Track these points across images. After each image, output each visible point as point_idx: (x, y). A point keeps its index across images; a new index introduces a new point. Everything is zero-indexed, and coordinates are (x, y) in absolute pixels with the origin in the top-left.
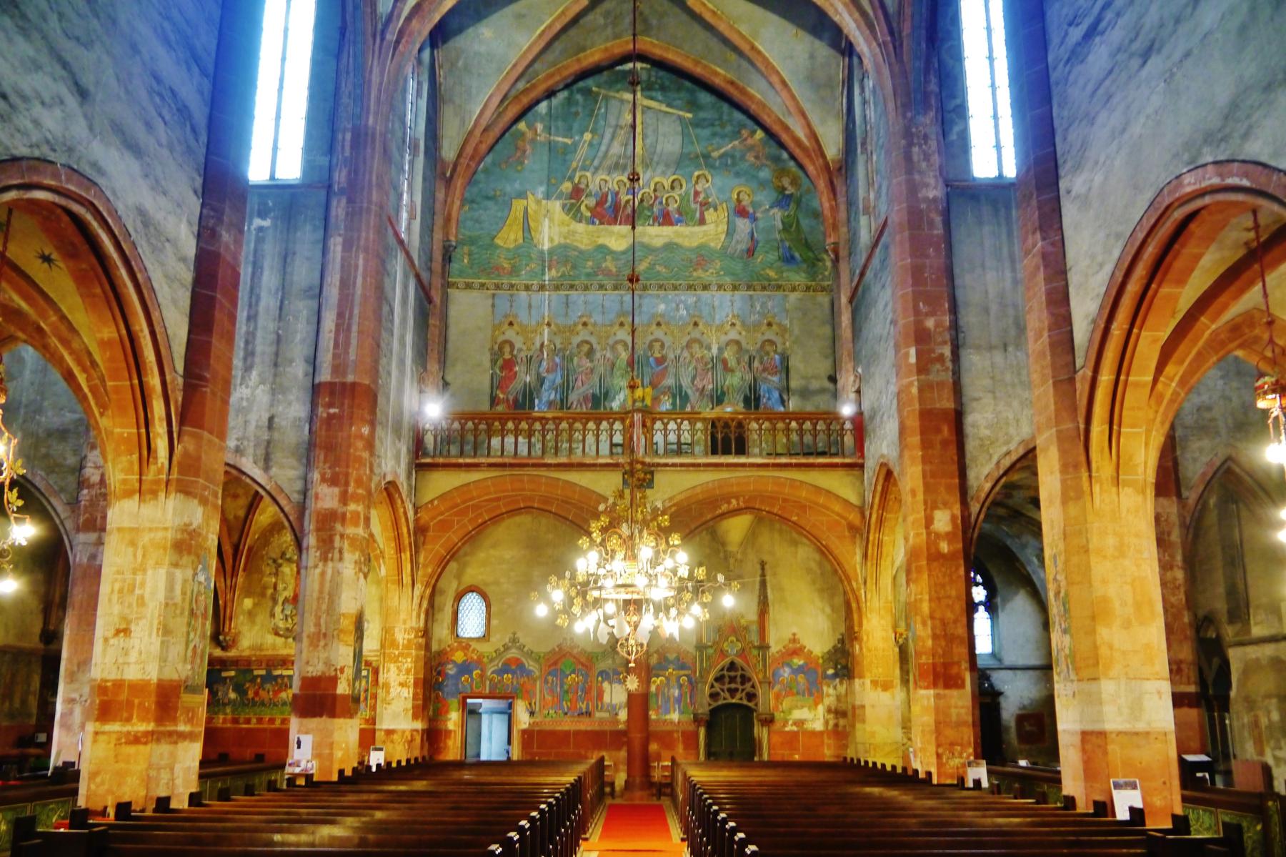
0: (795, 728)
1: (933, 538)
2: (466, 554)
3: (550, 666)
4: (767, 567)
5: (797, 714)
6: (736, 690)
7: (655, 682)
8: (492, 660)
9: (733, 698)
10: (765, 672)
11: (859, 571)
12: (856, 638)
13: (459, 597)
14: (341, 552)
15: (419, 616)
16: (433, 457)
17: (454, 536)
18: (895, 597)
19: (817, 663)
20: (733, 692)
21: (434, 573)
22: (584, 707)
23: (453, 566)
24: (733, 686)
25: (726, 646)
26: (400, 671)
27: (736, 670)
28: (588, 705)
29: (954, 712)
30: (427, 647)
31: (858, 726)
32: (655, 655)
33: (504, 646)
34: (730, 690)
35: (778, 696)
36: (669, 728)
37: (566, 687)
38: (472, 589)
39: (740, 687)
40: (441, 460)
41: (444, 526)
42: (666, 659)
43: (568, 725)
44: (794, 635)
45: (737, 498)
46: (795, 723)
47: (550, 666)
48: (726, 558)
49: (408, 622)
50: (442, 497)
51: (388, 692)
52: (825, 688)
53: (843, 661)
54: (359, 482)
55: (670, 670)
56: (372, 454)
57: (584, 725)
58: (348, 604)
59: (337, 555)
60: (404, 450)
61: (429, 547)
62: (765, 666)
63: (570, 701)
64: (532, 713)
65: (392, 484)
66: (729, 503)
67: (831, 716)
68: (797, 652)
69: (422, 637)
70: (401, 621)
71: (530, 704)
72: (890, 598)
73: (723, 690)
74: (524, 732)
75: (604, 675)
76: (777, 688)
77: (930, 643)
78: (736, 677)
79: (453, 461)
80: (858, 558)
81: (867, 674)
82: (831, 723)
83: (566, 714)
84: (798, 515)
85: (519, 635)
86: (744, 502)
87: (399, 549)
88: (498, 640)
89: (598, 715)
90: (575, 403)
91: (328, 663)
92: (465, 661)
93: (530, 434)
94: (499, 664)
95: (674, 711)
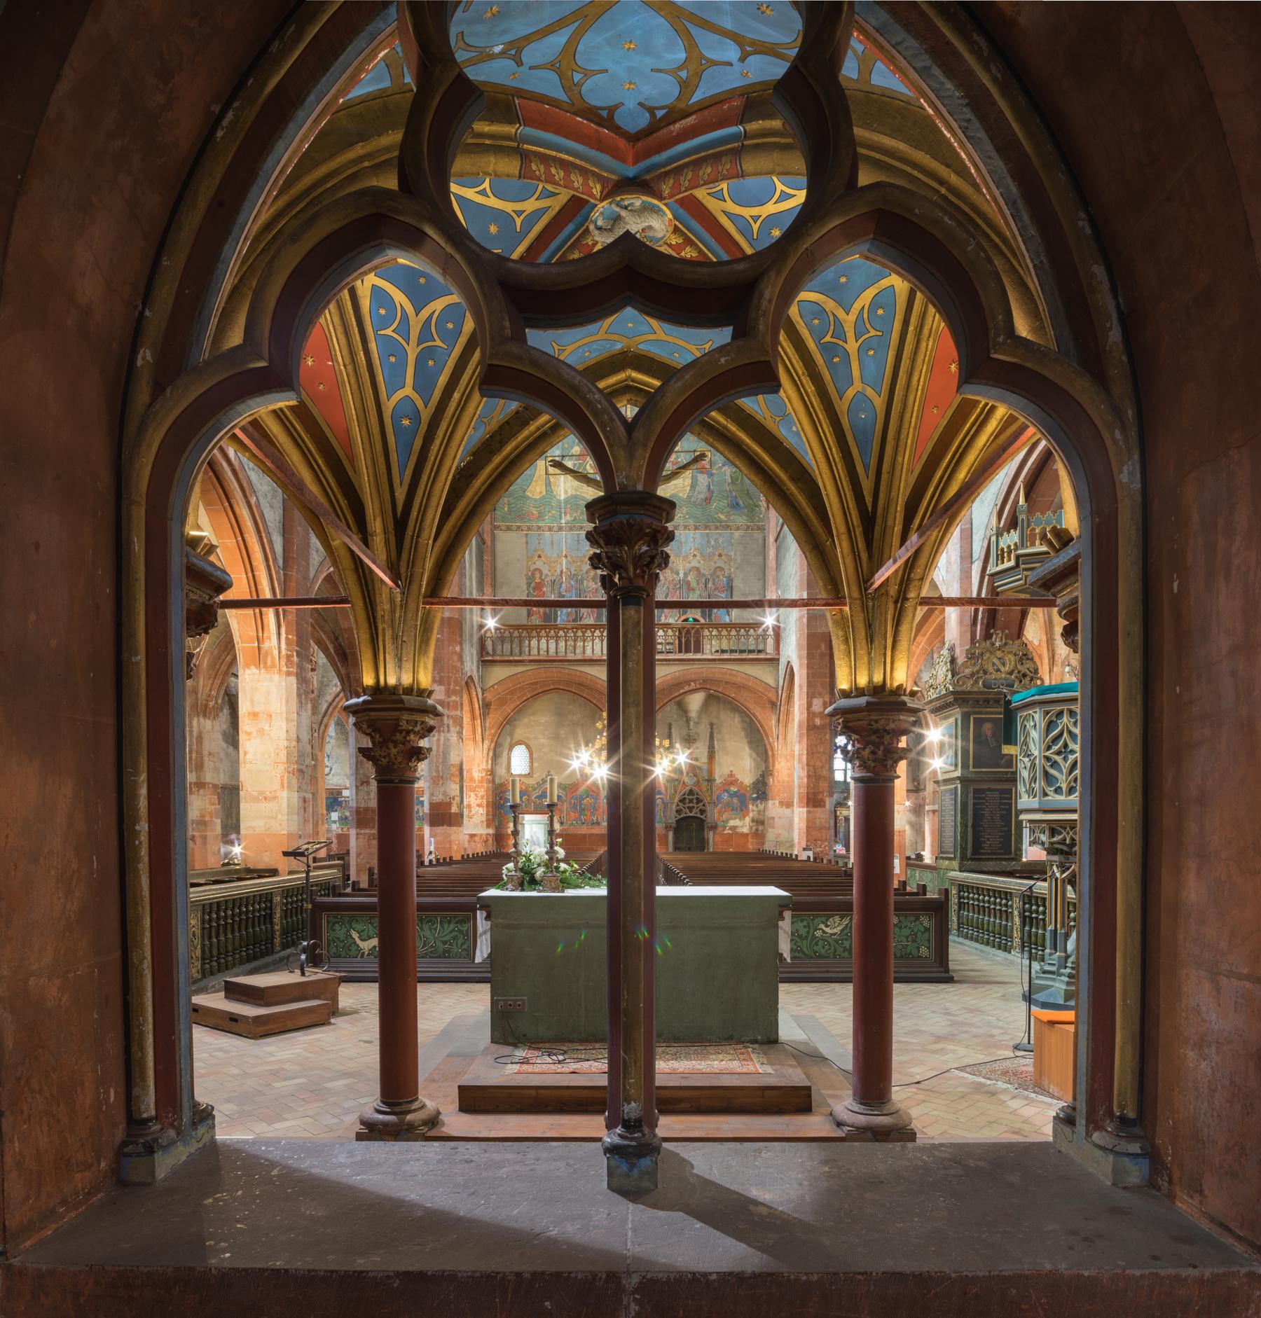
1: (811, 715)
2: (515, 720)
5: (732, 823)
10: (711, 796)
13: (511, 749)
14: (448, 726)
15: (487, 761)
16: (493, 655)
17: (508, 709)
20: (691, 809)
21: (496, 732)
23: (507, 726)
29: (818, 821)
35: (719, 812)
38: (520, 743)
40: (498, 658)
41: (502, 702)
43: (584, 830)
51: (470, 811)
53: (762, 789)
54: (456, 683)
56: (462, 662)
58: (454, 759)
59: (446, 728)
60: (475, 653)
61: (491, 716)
64: (562, 823)
65: (471, 677)
76: (720, 806)
77: (806, 780)
79: (507, 658)
80: (774, 722)
82: (754, 828)
87: (473, 718)
88: (538, 776)
91: (445, 794)
93: (557, 638)
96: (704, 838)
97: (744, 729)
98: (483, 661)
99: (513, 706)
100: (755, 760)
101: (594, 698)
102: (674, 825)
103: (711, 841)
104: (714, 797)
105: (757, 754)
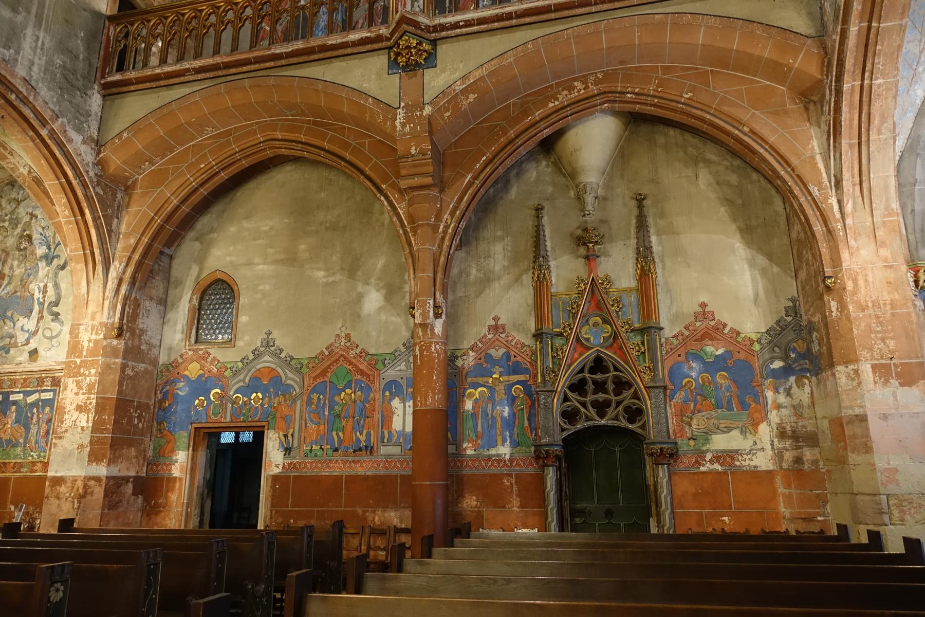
0: (717, 467)
2: (212, 230)
3: (315, 379)
4: (647, 203)
5: (720, 442)
6: (607, 404)
7: (471, 395)
8: (236, 374)
9: (602, 415)
11: (821, 166)
12: (828, 288)
18: (903, 207)
19: (751, 352)
20: (601, 408)
22: (363, 438)
24: (601, 396)
25: (585, 333)
26: (80, 388)
27: (605, 370)
28: (369, 434)
30: (132, 353)
31: (853, 458)
32: (471, 353)
33: (253, 352)
34: (595, 404)
35: (681, 413)
36: (494, 470)
37: (337, 408)
39: (614, 399)
42: (489, 357)
43: (338, 468)
44: (703, 305)
45: (584, 80)
46: (717, 458)
47: (315, 379)
48: (579, 198)
49: (98, 315)
50: (135, 127)
52: (769, 394)
53: (800, 346)
55: (494, 376)
57: (365, 467)
61: (133, 209)
62: (653, 360)
63: (343, 429)
64: (288, 451)
66: (571, 88)
67: (788, 443)
68: (715, 332)
69: (119, 336)
70: (89, 316)
71: (285, 436)
72: (895, 205)
73: (584, 405)
74: (275, 478)
75: (394, 388)
76: (680, 396)
78: (605, 383)
81: (865, 354)
82: (789, 456)
83: (336, 450)
84: (692, 90)
85: (275, 334)
86: (597, 82)
89: (383, 450)
90: (361, 21)
92: (201, 376)
94: (245, 378)
95: (504, 442)
96: (647, 487)
97: (728, 201)
98: (106, 86)
99: (177, 183)
100: (764, 272)
101: (346, 146)
102: (558, 450)
103: (664, 493)
104: (663, 373)
105: (770, 256)
